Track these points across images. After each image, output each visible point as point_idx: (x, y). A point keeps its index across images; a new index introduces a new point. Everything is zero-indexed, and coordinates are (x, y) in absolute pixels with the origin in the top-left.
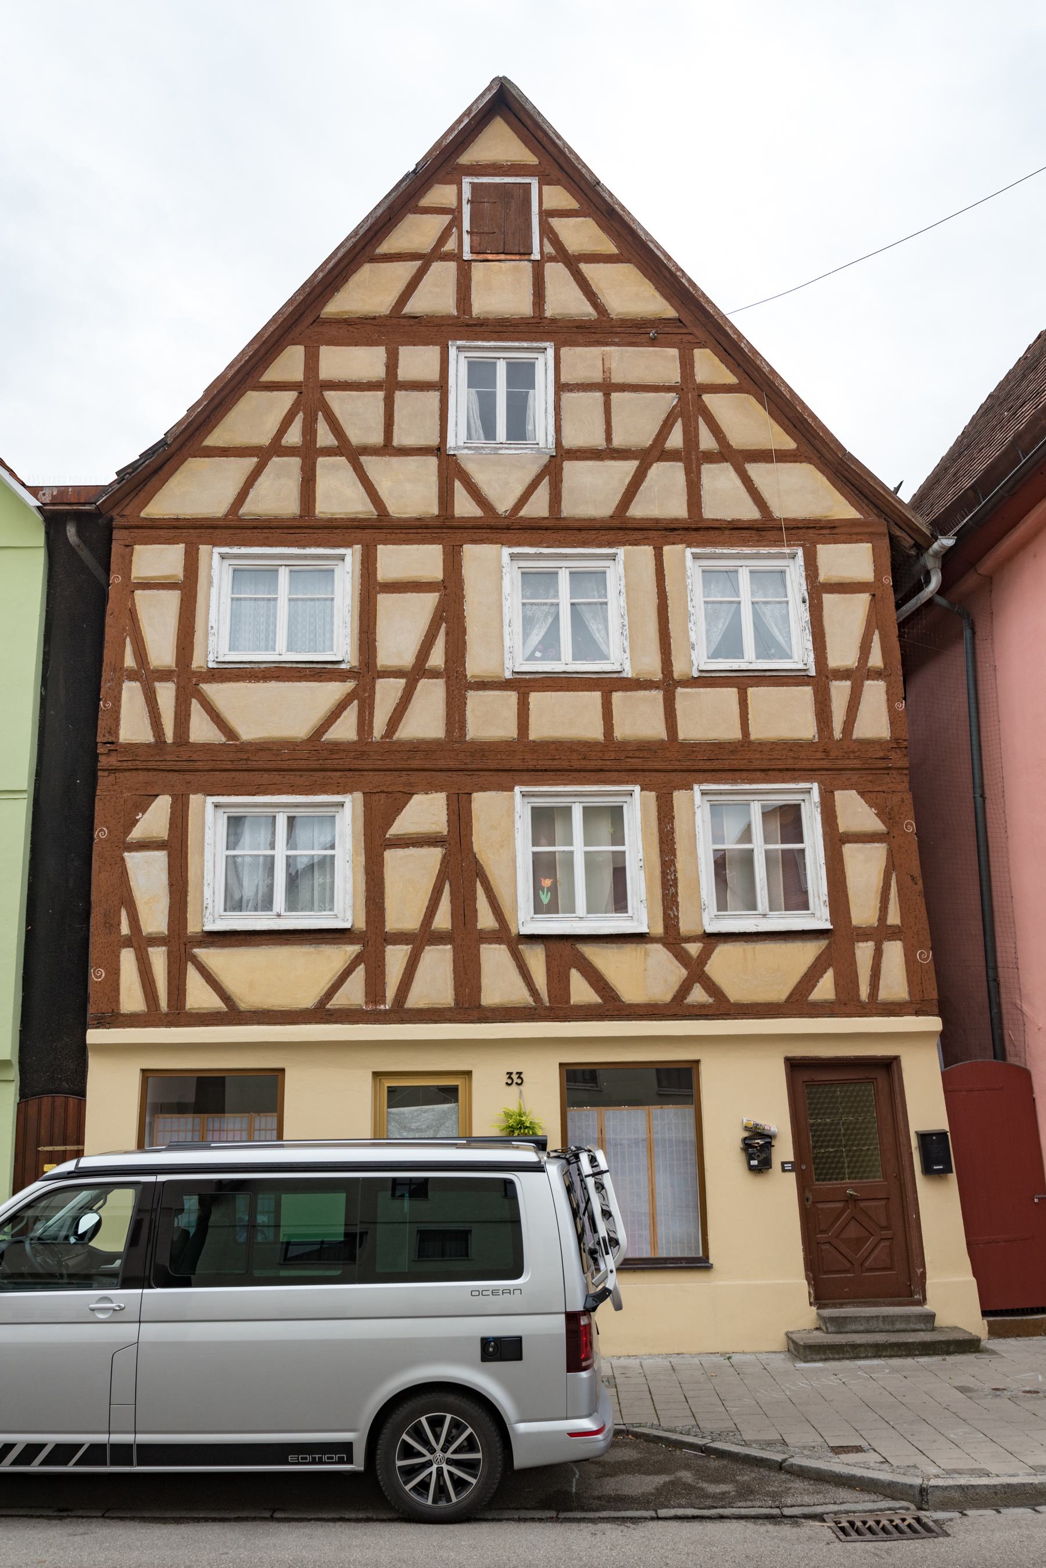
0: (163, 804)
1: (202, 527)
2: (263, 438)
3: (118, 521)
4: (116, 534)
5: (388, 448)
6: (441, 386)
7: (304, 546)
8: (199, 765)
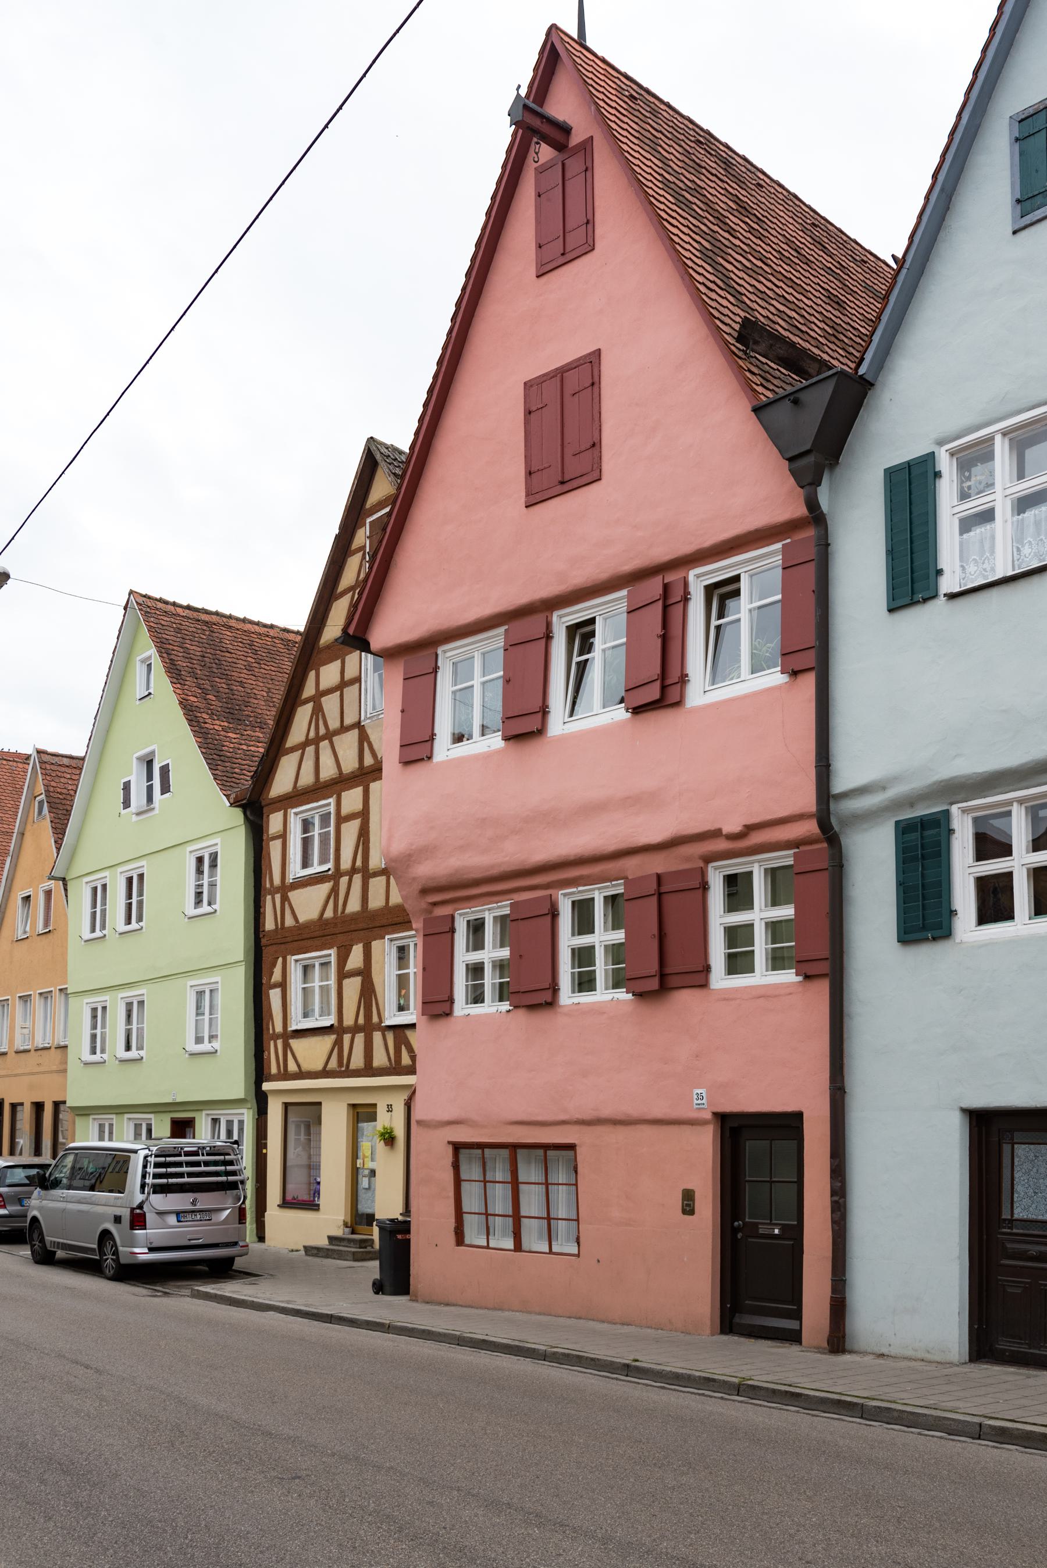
0: (280, 960)
1: (287, 799)
2: (302, 738)
3: (263, 803)
4: (265, 810)
5: (343, 729)
6: (358, 680)
7: (317, 801)
8: (289, 939)
